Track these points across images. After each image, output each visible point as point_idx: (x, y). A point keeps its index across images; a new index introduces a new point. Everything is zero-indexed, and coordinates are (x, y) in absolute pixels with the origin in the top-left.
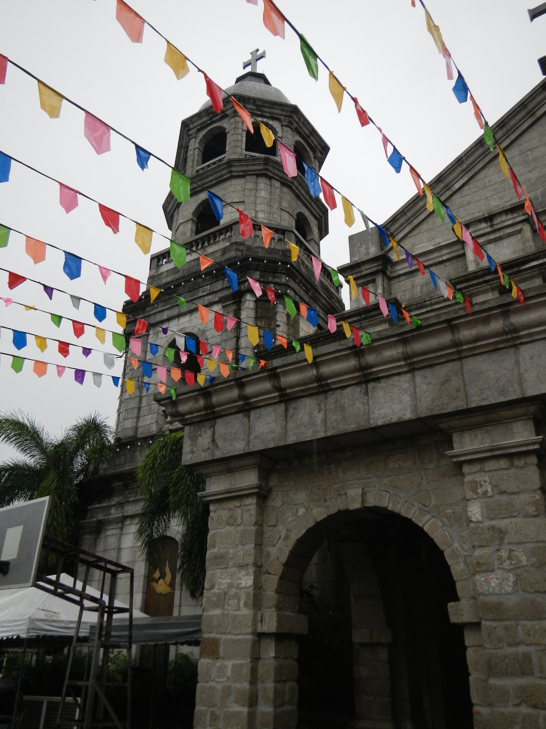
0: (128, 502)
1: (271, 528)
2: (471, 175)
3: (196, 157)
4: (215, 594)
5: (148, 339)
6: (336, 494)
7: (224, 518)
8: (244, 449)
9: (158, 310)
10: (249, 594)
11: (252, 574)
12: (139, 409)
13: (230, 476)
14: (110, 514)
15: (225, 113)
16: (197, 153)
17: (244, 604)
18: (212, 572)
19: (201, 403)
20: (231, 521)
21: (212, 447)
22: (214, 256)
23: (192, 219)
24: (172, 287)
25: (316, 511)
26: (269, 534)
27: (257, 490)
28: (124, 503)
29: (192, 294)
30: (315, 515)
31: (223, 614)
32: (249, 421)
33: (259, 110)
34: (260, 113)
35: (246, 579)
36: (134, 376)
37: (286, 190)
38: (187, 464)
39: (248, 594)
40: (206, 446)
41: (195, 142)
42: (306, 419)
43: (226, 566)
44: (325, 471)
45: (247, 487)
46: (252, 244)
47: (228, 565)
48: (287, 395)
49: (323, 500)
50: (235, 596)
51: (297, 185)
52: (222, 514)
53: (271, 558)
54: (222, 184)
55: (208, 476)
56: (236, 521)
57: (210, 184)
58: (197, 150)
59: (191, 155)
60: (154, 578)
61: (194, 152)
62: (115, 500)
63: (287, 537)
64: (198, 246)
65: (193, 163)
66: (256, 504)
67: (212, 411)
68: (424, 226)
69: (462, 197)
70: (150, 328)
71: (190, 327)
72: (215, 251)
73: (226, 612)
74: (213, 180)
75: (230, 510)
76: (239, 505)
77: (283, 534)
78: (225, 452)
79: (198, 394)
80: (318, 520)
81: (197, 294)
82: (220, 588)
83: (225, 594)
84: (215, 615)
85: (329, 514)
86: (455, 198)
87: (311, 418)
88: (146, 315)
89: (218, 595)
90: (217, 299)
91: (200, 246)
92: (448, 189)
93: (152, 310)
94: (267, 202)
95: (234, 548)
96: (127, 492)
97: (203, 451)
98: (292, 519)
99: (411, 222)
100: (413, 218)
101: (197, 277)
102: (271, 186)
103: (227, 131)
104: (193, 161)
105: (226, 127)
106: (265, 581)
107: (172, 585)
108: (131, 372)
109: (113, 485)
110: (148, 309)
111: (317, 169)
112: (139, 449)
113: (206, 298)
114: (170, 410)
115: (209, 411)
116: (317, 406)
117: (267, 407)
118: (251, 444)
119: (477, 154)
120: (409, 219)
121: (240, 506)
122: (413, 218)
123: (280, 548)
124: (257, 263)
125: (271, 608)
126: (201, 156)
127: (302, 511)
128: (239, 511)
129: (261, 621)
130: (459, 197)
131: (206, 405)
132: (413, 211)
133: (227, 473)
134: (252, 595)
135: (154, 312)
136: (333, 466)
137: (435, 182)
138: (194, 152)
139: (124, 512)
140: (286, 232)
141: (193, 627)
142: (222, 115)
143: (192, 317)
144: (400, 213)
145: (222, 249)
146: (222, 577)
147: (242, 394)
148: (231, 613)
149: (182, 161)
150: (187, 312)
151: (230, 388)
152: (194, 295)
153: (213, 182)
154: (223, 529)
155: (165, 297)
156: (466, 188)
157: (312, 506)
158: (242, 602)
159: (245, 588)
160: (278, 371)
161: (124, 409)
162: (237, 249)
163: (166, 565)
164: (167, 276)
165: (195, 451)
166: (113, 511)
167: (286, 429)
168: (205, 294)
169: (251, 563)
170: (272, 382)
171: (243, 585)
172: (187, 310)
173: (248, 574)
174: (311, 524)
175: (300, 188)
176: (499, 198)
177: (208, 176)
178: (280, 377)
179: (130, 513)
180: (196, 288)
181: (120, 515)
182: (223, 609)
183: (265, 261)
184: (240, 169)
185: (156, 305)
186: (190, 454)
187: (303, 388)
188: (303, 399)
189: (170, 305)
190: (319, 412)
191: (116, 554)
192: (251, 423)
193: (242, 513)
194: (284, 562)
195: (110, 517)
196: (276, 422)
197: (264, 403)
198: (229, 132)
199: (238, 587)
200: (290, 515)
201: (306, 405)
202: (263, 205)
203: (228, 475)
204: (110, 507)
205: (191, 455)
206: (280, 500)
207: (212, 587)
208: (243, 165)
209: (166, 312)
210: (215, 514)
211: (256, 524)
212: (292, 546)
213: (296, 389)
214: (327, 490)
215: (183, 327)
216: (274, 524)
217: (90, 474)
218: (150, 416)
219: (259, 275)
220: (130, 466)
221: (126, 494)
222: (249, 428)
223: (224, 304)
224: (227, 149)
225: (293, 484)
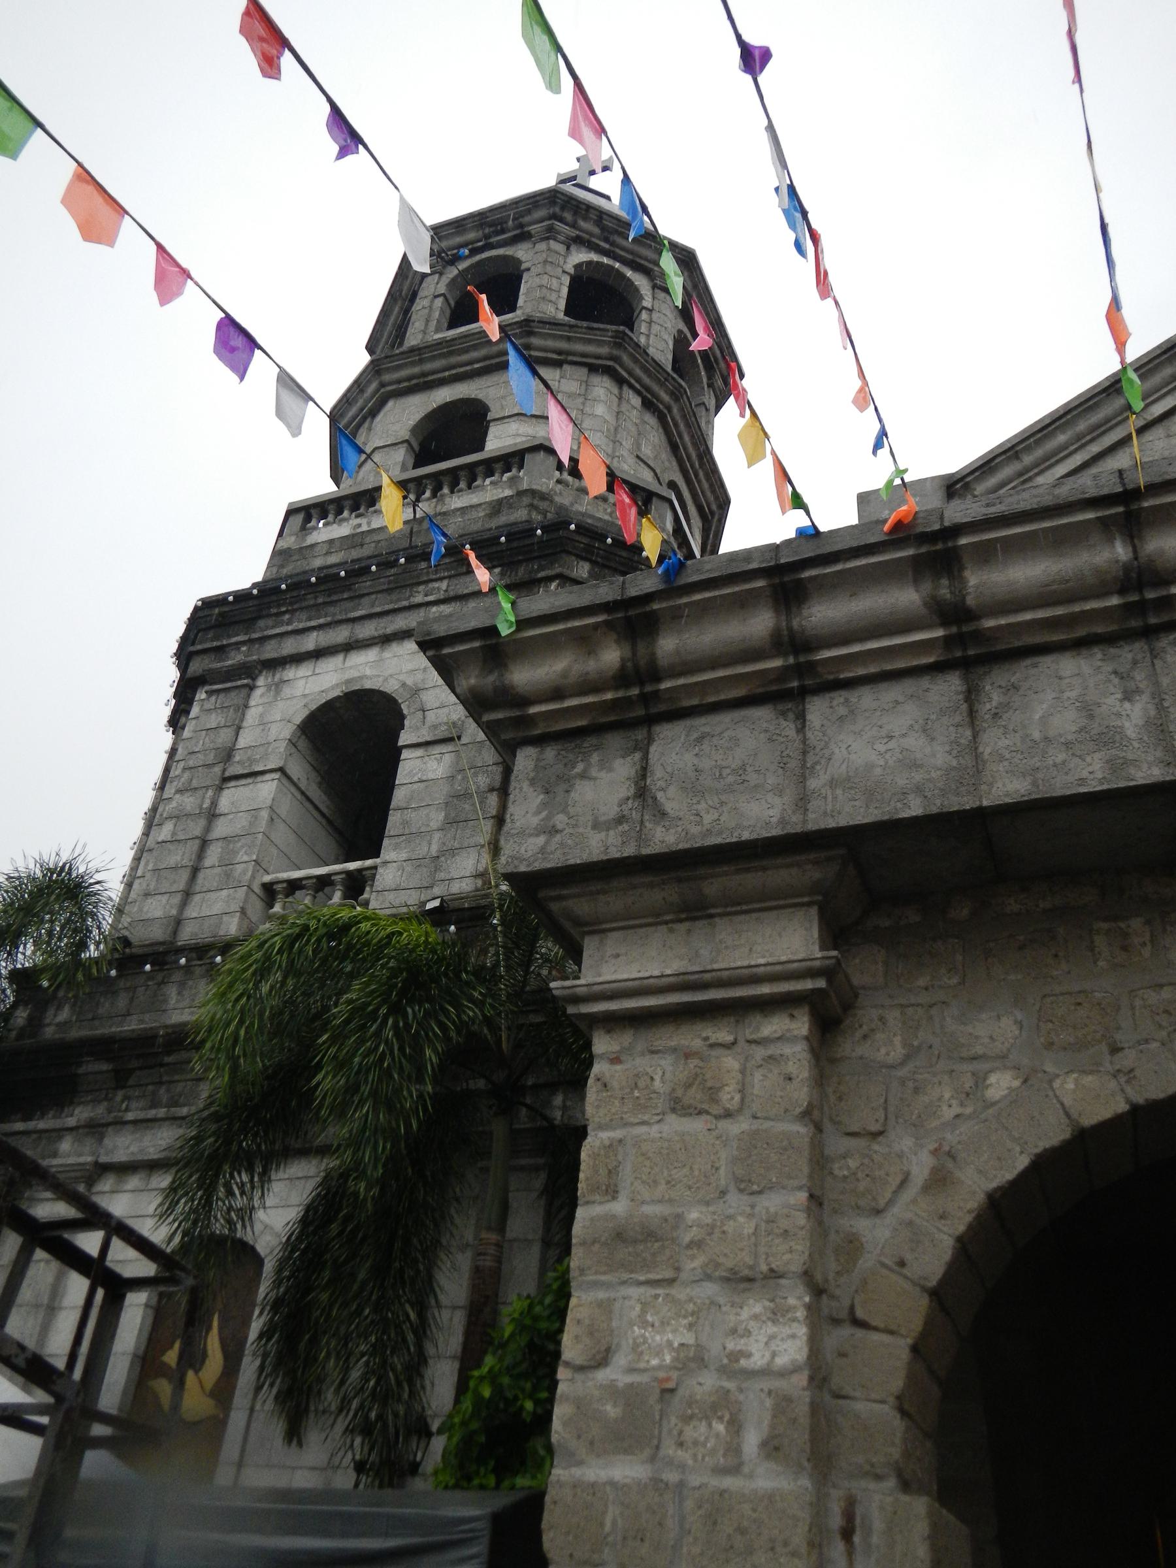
0: (120, 1123)
1: (861, 1143)
3: (437, 314)
4: (612, 1391)
5: (249, 696)
6: (1160, 1026)
7: (657, 1083)
8: (783, 821)
9: (290, 628)
10: (788, 1399)
11: (801, 1314)
12: (195, 871)
13: (689, 931)
14: (55, 1155)
15: (526, 229)
16: (440, 305)
17: (764, 1444)
18: (602, 1295)
19: (611, 656)
20: (694, 1096)
21: (635, 815)
22: (466, 517)
23: (407, 441)
24: (343, 573)
25: (1070, 1086)
26: (852, 1163)
27: (821, 983)
28: (108, 1125)
29: (394, 596)
30: (1067, 1102)
31: (657, 1483)
32: (801, 729)
33: (606, 240)
34: (607, 246)
35: (772, 1337)
36: (195, 783)
37: (652, 420)
38: (523, 868)
39: (783, 1403)
40: (610, 810)
41: (437, 283)
42: (1067, 722)
43: (668, 1274)
44: (1100, 941)
45: (778, 968)
46: (572, 504)
47: (678, 1269)
48: (979, 636)
49: (1104, 1048)
50: (714, 1407)
51: (678, 418)
52: (649, 1070)
53: (867, 1262)
54: (501, 372)
55: (596, 927)
56: (714, 1100)
57: (468, 368)
58: (440, 300)
59: (424, 308)
60: (165, 1364)
61: (432, 302)
62: (79, 1114)
63: (939, 1180)
65: (427, 325)
66: (807, 1038)
67: (649, 688)
69: (1169, 436)
70: (261, 672)
71: (379, 676)
72: (472, 507)
73: (672, 1477)
74: (478, 361)
75: (687, 1056)
76: (730, 1038)
77: (921, 1166)
78: (695, 830)
79: (606, 622)
80: (1088, 1121)
82: (642, 1365)
83: (667, 1392)
84: (612, 1483)
85: (1140, 1100)
86: (1151, 438)
87: (1091, 717)
88: (255, 636)
89: (630, 1397)
91: (428, 494)
93: (273, 627)
94: (608, 430)
95: (707, 1204)
96: (120, 1095)
97: (596, 826)
98: (959, 1110)
99: (1030, 479)
100: (1036, 471)
101: (417, 556)
102: (620, 398)
103: (524, 266)
104: (427, 321)
105: (523, 259)
106: (843, 1355)
107: (223, 1392)
108: (187, 775)
109: (81, 1071)
110: (261, 623)
111: (712, 408)
112: (177, 976)
113: (434, 609)
114: (473, 681)
115: (635, 691)
116: (1116, 681)
117: (883, 686)
118: (814, 804)
120: (1027, 470)
121: (734, 1043)
122: (1036, 471)
123: (910, 1223)
124: (585, 540)
125: (879, 1478)
126: (448, 312)
127: (1001, 1084)
128: (731, 1062)
129: (847, 1534)
130: (1162, 436)
131: (629, 664)
132: (1039, 453)
133: (681, 921)
134: (802, 1409)
135: (277, 631)
136: (1136, 923)
137: (1105, 390)
138: (432, 302)
139: (102, 1151)
140: (654, 500)
141: (386, 1535)
142: (517, 232)
143: (387, 654)
144: (1004, 452)
145: (490, 503)
146: (649, 1318)
147: (790, 629)
148: (694, 1480)
149: (399, 313)
150: (374, 638)
151: (743, 604)
152: (399, 600)
153: (476, 366)
154: (656, 1128)
155: (316, 598)
157: (1050, 1068)
158: (751, 1441)
159: (765, 1372)
160: (963, 541)
161: (150, 867)
162: (532, 506)
163: (209, 1328)
164: (328, 553)
165: (559, 826)
166: (66, 1145)
167: (977, 756)
168: (431, 598)
169: (796, 1266)
170: (927, 586)
171: (758, 1359)
173: (777, 1314)
174: (1054, 1134)
175: (682, 426)
177: (466, 351)
178: (962, 568)
179: (120, 1156)
180: (408, 585)
181: (89, 1159)
182: (653, 1459)
183: (609, 541)
184: (550, 343)
185: (287, 616)
186: (537, 835)
187: (1059, 611)
188: (1047, 661)
189: (329, 619)
190: (1128, 696)
191: (50, 1279)
192: (809, 734)
193: (743, 1072)
194: (933, 1282)
195: (55, 1162)
196: (924, 731)
197: (873, 669)
198: (528, 269)
199: (732, 1367)
200: (947, 1095)
201: (1060, 678)
202: (599, 434)
203: (686, 925)
204: (59, 1133)
205: (541, 840)
206: (897, 1040)
207: (602, 1360)
208: (561, 337)
209: (315, 634)
210: (618, 1067)
211: (806, 1114)
212: (969, 1218)
213: (1028, 616)
214: (1119, 1009)
215: (356, 674)
216: (874, 1128)
217: (14, 1034)
218: (225, 893)
219: (589, 573)
220: (142, 1021)
221: (119, 1098)
222: (804, 753)
224: (520, 302)
225: (955, 981)
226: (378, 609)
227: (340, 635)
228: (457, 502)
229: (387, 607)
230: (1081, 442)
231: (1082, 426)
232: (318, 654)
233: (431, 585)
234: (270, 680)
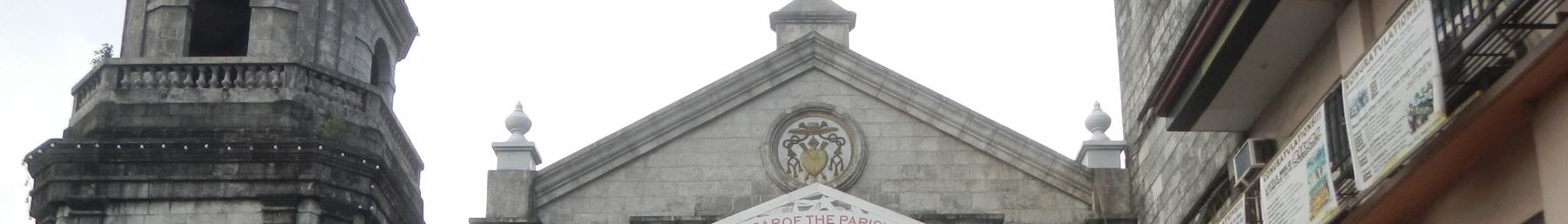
2: (662, 142)
64: (211, 77)
68: (592, 191)
70: (108, 206)
81: (211, 173)
88: (101, 178)
90: (253, 195)
91: (214, 78)
92: (631, 151)
99: (577, 178)
113: (231, 185)
119: (674, 119)
156: (652, 157)
162: (292, 115)
168: (229, 178)
172: (192, 195)
176: (689, 189)
185: (122, 167)
189: (156, 177)
223: (268, 208)
226: (192, 178)
227: (166, 190)
228: (238, 95)
229: (200, 177)
230: (604, 162)
231: (605, 154)
232: (150, 200)
233: (228, 165)
234: (116, 211)
